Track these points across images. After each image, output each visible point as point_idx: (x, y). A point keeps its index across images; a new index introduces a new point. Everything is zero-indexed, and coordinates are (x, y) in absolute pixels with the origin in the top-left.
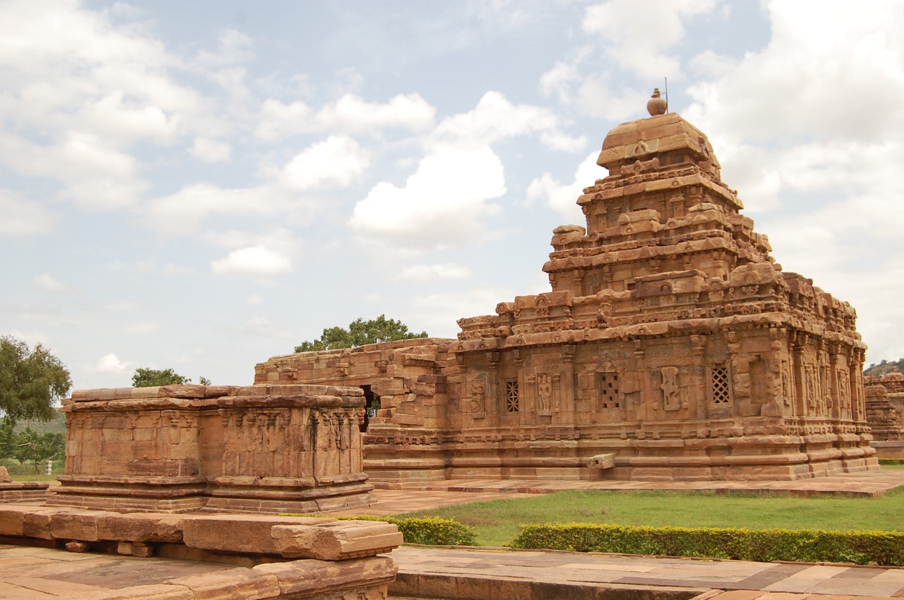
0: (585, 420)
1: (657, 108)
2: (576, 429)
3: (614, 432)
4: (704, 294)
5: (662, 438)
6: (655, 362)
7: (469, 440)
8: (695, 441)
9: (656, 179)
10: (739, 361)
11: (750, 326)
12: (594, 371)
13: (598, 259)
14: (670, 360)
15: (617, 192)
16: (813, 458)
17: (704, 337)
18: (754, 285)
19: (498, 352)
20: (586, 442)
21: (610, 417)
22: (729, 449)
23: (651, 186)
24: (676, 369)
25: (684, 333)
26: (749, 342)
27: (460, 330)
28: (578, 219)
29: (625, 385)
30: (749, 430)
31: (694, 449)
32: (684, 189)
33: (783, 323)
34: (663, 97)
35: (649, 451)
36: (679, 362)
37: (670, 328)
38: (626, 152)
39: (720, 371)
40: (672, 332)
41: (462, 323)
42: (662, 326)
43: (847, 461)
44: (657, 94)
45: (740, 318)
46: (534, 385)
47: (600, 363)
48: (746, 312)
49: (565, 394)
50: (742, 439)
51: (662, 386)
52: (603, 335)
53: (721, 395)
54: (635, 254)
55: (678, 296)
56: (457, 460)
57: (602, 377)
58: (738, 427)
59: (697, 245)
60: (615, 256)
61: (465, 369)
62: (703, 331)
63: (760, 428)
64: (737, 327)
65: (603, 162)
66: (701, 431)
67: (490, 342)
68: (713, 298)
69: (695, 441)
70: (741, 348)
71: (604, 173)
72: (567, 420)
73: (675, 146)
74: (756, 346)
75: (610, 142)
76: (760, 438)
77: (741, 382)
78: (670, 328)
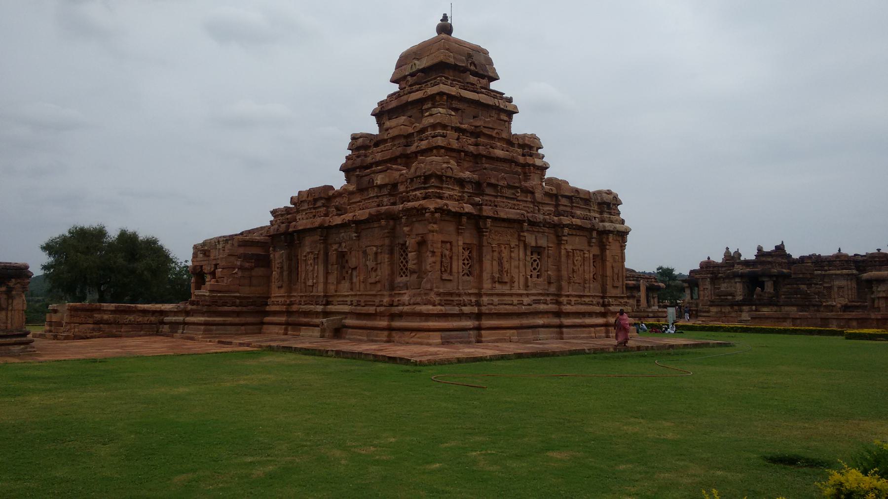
2: (325, 296)
3: (345, 299)
4: (395, 186)
5: (366, 305)
7: (274, 304)
8: (382, 309)
9: (417, 91)
10: (411, 242)
11: (415, 211)
12: (336, 250)
16: (483, 326)
17: (392, 223)
18: (420, 176)
19: (286, 234)
20: (330, 308)
22: (401, 315)
24: (375, 249)
26: (417, 225)
27: (272, 218)
28: (372, 128)
29: (353, 261)
30: (412, 301)
33: (436, 209)
34: (449, 22)
35: (359, 316)
36: (378, 243)
37: (370, 214)
38: (407, 70)
41: (274, 212)
43: (565, 330)
44: (445, 18)
45: (410, 204)
47: (340, 244)
48: (413, 200)
50: (406, 309)
51: (368, 263)
52: (338, 220)
54: (388, 155)
55: (380, 187)
56: (268, 319)
58: (406, 298)
63: (419, 299)
64: (408, 212)
65: (395, 78)
66: (386, 300)
68: (401, 188)
69: (382, 309)
70: (411, 230)
71: (395, 88)
73: (436, 61)
74: (419, 228)
76: (418, 308)
78: (370, 214)
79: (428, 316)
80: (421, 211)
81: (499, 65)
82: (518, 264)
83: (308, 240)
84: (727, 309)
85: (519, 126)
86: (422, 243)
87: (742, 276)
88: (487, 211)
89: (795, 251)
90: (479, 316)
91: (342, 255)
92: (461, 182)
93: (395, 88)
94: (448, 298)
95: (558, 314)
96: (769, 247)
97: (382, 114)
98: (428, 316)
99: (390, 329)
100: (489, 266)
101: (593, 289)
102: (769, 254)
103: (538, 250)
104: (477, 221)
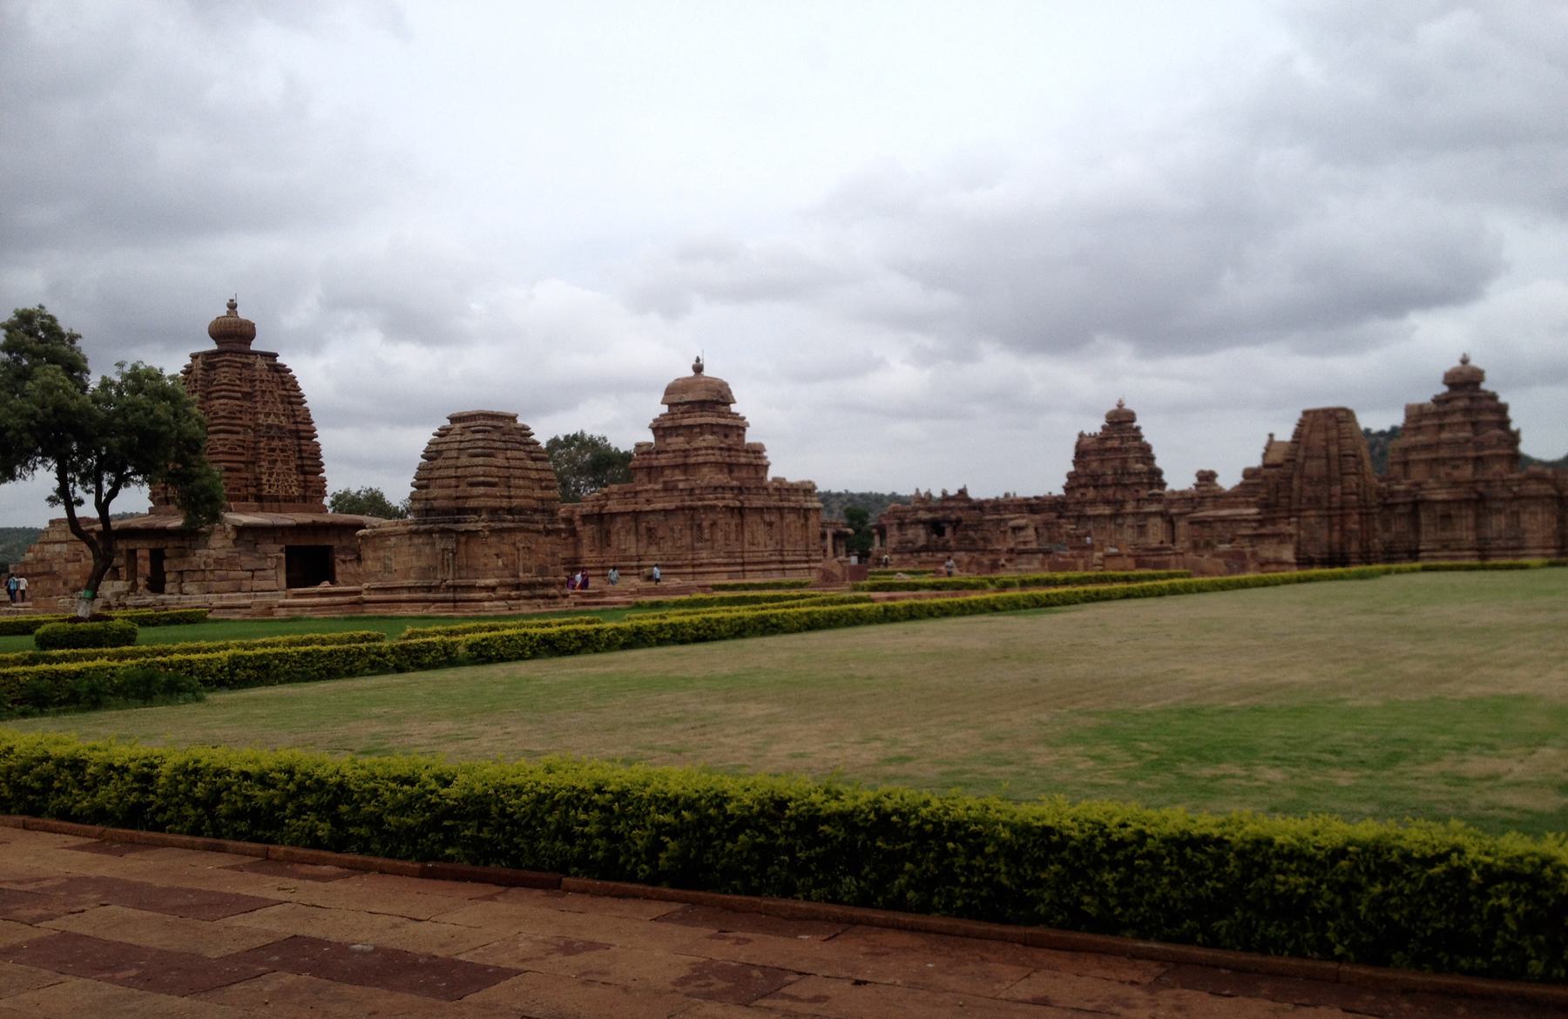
0: (642, 552)
1: (698, 369)
4: (692, 489)
6: (671, 523)
10: (706, 524)
13: (655, 463)
14: (678, 522)
15: (668, 424)
21: (653, 550)
22: (701, 565)
23: (686, 422)
25: (683, 509)
29: (660, 533)
31: (687, 566)
32: (700, 426)
39: (700, 526)
40: (677, 509)
42: (672, 506)
46: (618, 533)
49: (632, 538)
52: (648, 508)
53: (700, 539)
57: (649, 529)
59: (701, 459)
60: (663, 462)
61: (584, 524)
62: (691, 508)
64: (705, 507)
67: (596, 510)
72: (633, 551)
74: (712, 516)
75: (670, 391)
77: (707, 535)
79: (720, 565)
80: (713, 507)
81: (735, 394)
82: (761, 533)
83: (619, 520)
84: (907, 556)
85: (750, 437)
86: (714, 524)
87: (924, 522)
88: (747, 504)
89: (975, 494)
90: (743, 564)
91: (649, 529)
92: (732, 489)
93: (665, 409)
94: (730, 554)
95: (781, 562)
96: (952, 492)
97: (658, 428)
98: (720, 565)
99: (455, 601)
100: (747, 536)
101: (801, 547)
102: (953, 498)
103: (770, 524)
104: (741, 511)
